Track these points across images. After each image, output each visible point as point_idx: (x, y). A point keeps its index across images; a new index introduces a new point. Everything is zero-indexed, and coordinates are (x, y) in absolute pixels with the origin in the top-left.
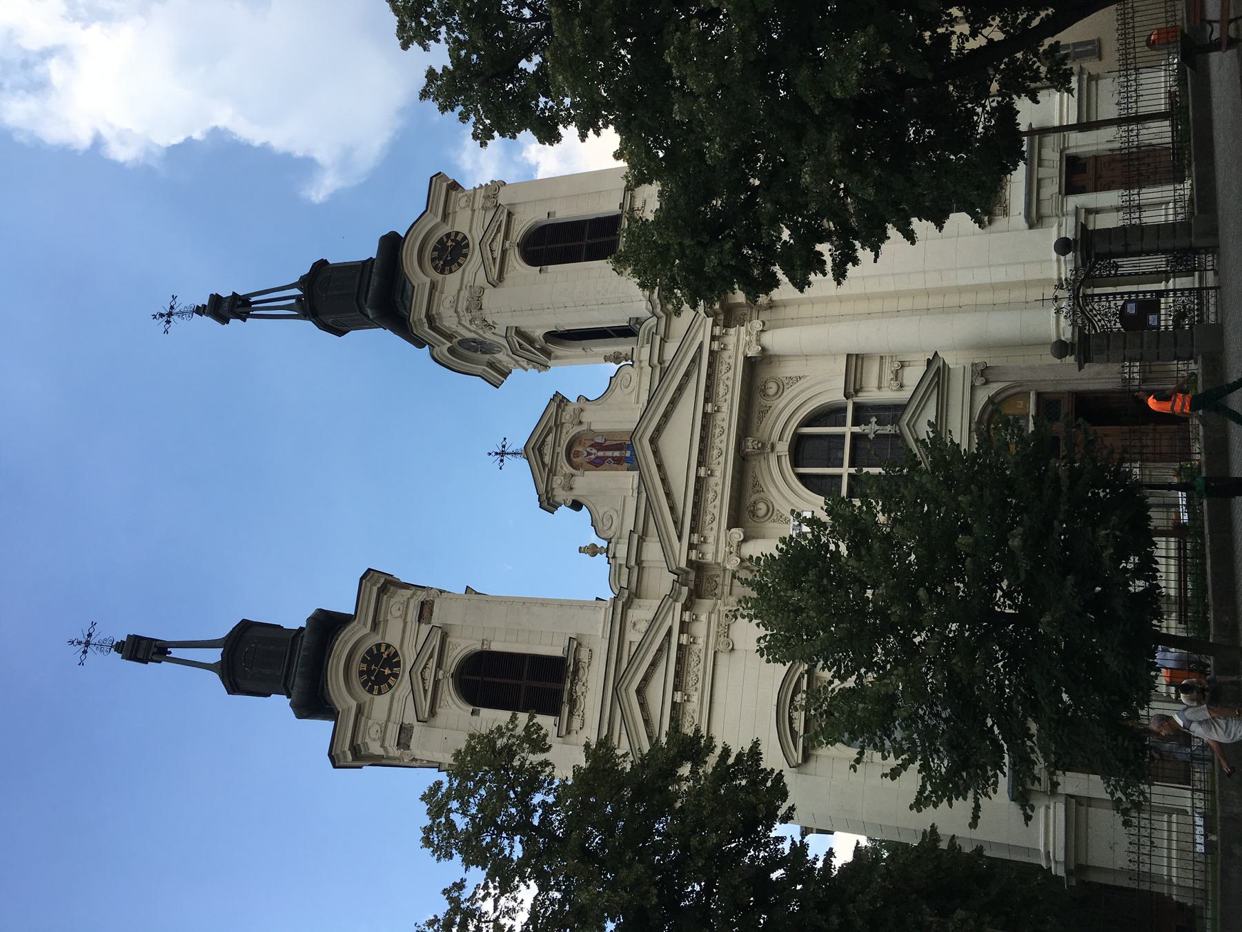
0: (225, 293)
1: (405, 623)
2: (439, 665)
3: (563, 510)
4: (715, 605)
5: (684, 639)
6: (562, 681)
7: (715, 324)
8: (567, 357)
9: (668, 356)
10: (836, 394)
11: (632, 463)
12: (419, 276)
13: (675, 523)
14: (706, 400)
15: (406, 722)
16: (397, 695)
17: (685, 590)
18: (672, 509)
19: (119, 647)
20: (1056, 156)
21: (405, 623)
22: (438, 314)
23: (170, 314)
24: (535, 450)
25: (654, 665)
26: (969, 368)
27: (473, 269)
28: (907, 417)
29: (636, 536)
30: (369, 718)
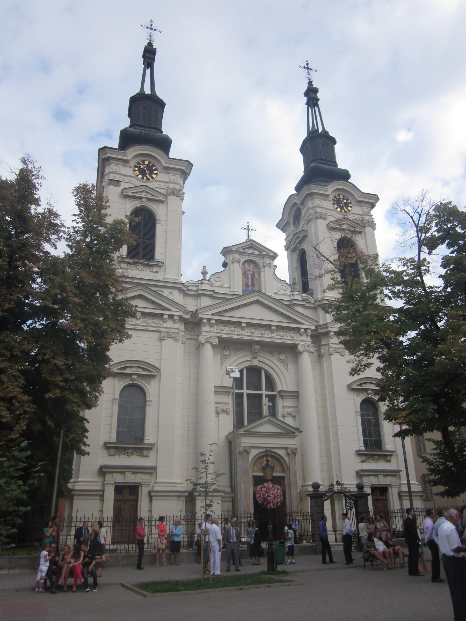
0: (319, 95)
1: (168, 183)
2: (149, 199)
3: (222, 259)
4: (182, 331)
6: (143, 258)
7: (312, 330)
8: (292, 259)
9: (297, 308)
10: (279, 388)
11: (246, 292)
12: (331, 188)
13: (220, 312)
14: (277, 327)
15: (121, 183)
16: (133, 179)
17: (188, 317)
18: (226, 311)
19: (150, 44)
20: (388, 482)
21: (168, 183)
22: (314, 198)
23: (308, 68)
24: (251, 245)
26: (295, 446)
27: (334, 214)
28: (273, 419)
29: (212, 293)
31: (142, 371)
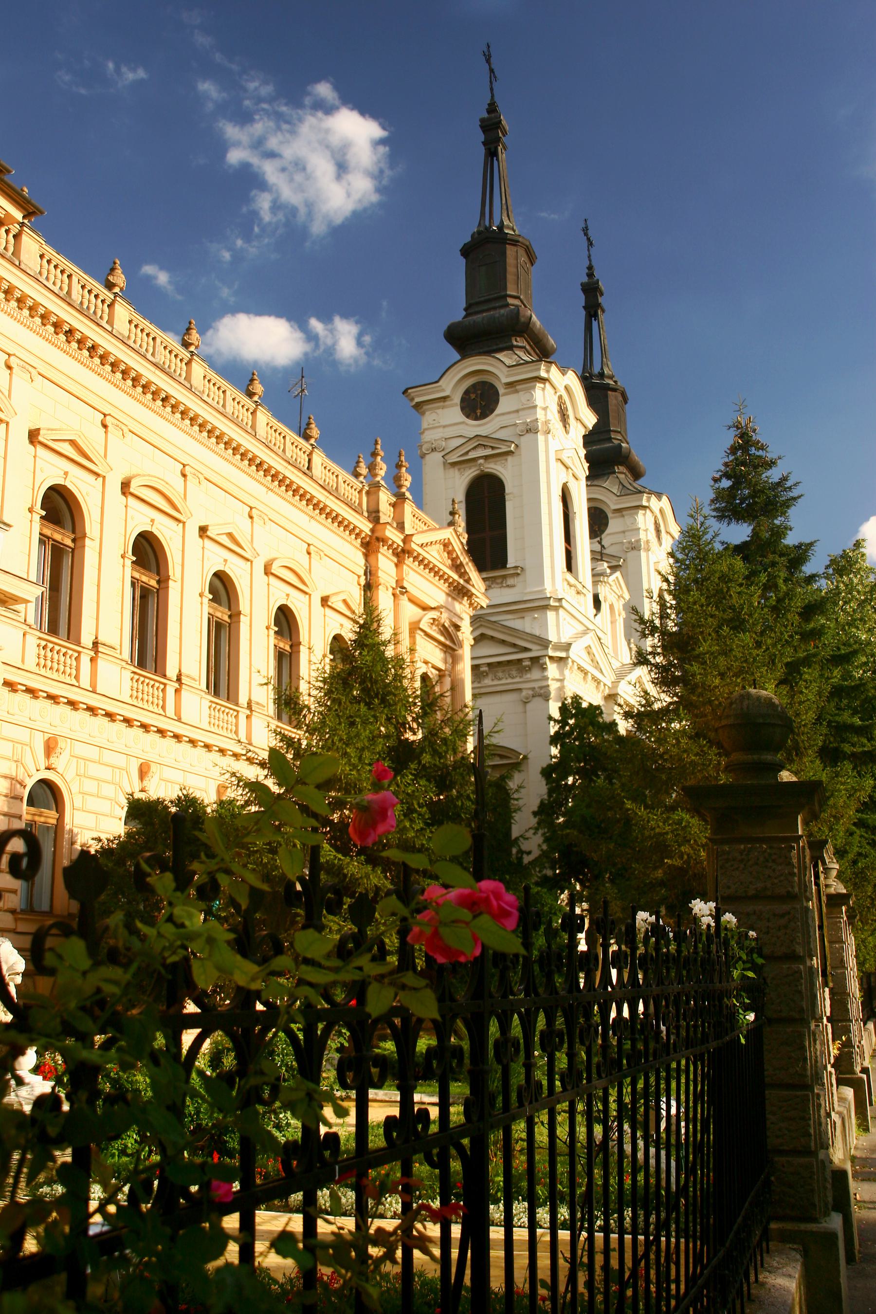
2: (486, 458)
5: (527, 663)
16: (461, 426)
19: (492, 108)
25: (503, 642)
30: (443, 407)
31: (498, 758)
